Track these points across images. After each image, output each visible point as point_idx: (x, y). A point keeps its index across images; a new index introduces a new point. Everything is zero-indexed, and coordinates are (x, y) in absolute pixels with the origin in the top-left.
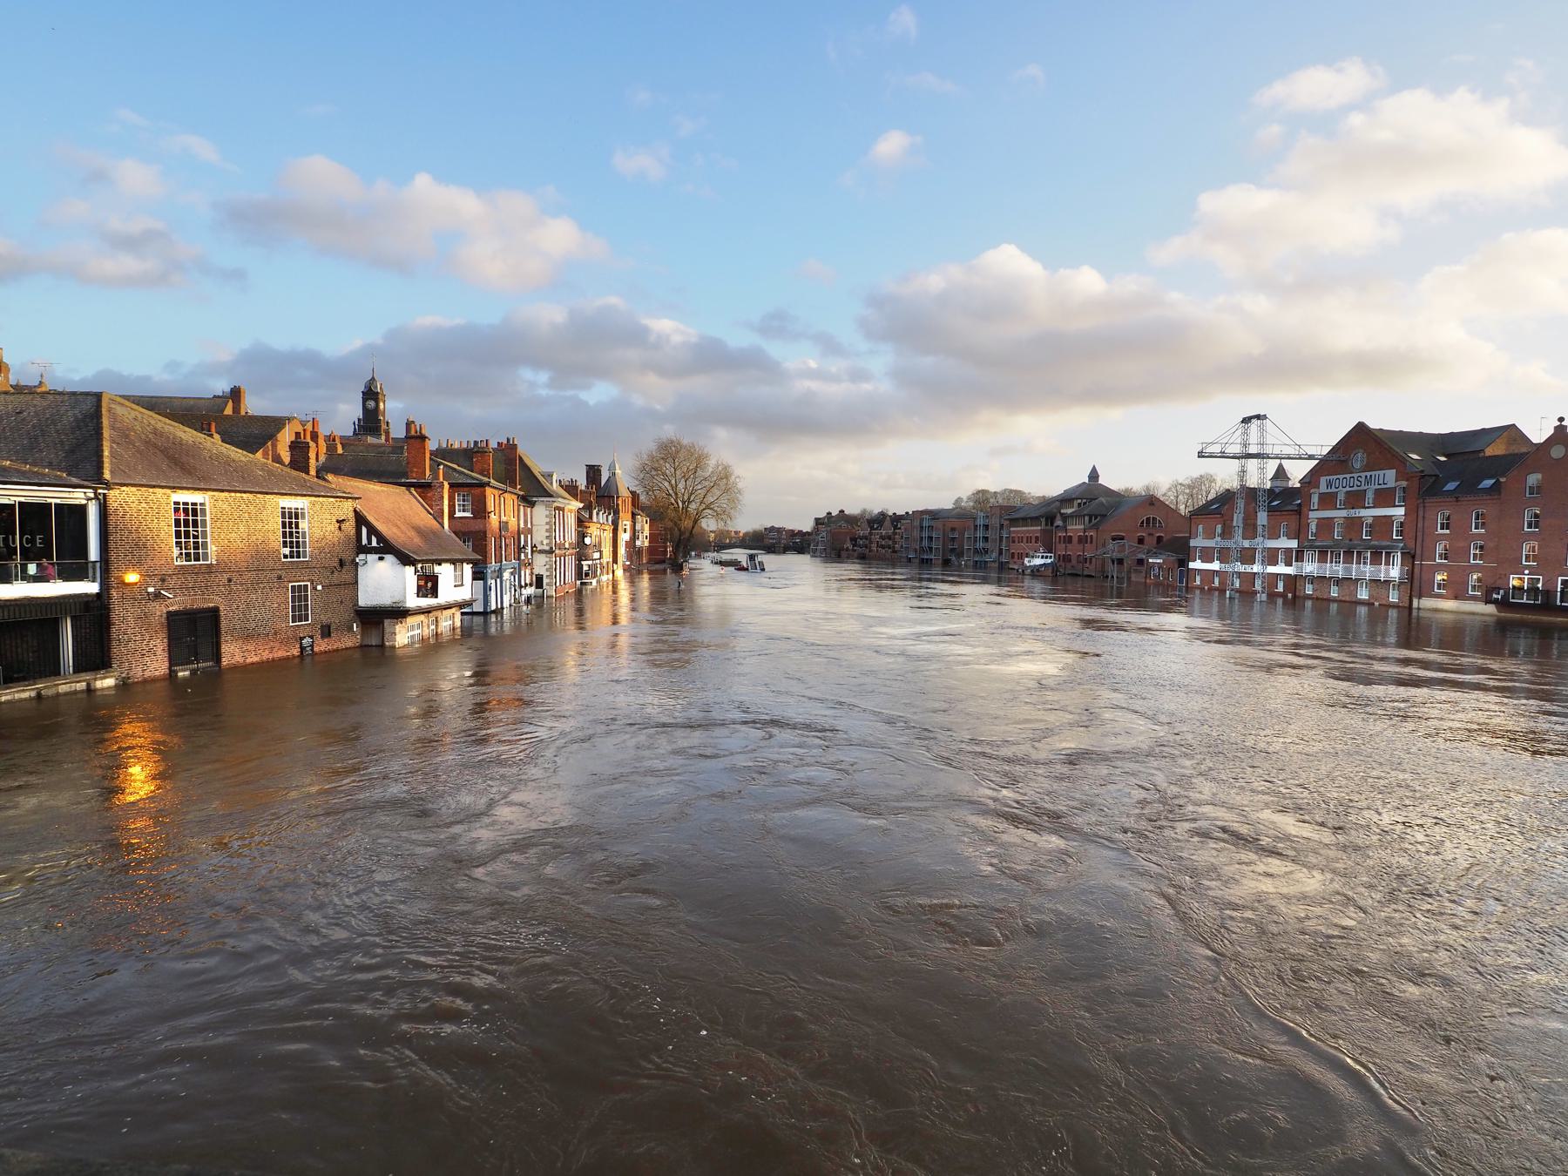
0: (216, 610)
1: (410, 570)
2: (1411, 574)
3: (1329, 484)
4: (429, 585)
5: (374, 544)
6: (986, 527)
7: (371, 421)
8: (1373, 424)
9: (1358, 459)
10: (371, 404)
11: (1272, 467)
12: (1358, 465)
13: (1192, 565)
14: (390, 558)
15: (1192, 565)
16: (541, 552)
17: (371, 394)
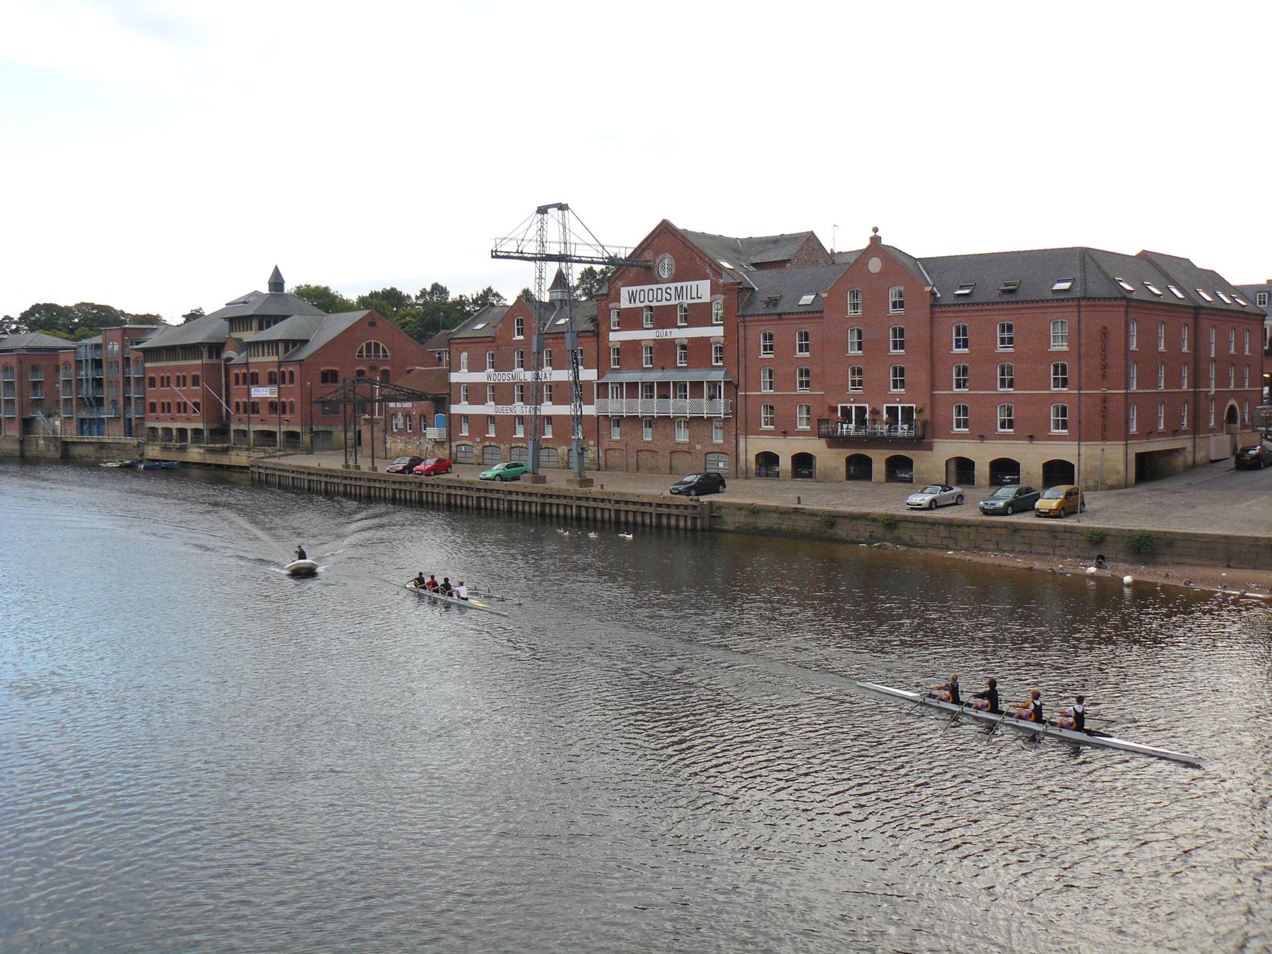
2: (734, 407)
3: (632, 297)
6: (98, 364)
8: (680, 224)
9: (666, 266)
11: (552, 268)
12: (665, 275)
13: (455, 409)
15: (455, 409)
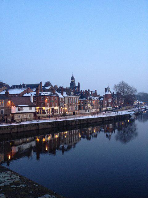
7: (72, 84)
10: (72, 81)
17: (73, 78)
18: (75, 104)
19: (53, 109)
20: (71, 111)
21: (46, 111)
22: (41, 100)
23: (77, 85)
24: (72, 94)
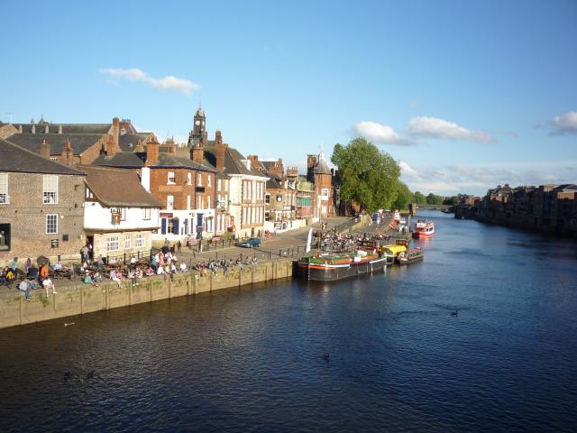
0: (9, 224)
1: (107, 211)
4: (116, 218)
5: (92, 197)
7: (198, 133)
10: (198, 123)
14: (97, 204)
16: (234, 205)
17: (198, 117)
18: (257, 202)
19: (200, 216)
20: (247, 227)
21: (181, 225)
22: (165, 183)
23: (211, 137)
24: (249, 167)
